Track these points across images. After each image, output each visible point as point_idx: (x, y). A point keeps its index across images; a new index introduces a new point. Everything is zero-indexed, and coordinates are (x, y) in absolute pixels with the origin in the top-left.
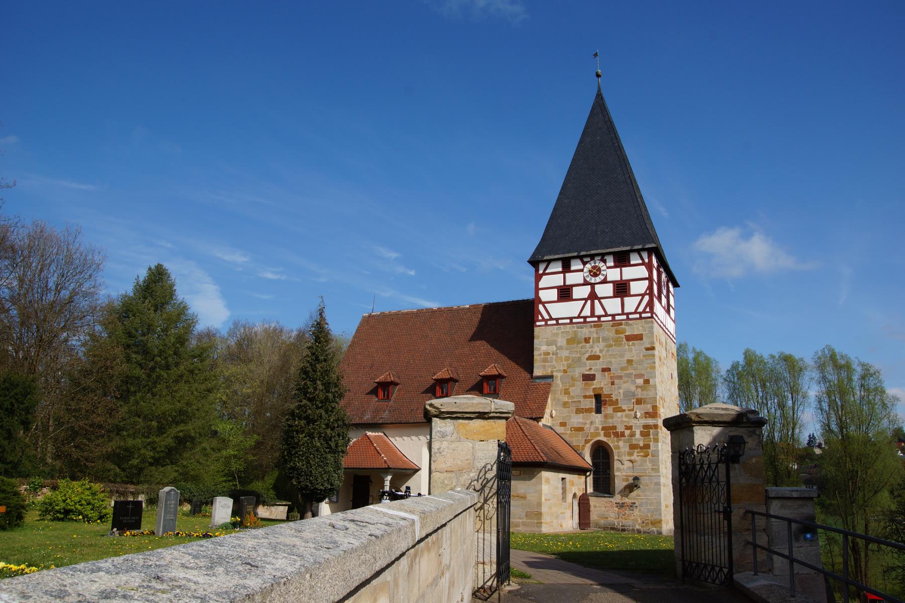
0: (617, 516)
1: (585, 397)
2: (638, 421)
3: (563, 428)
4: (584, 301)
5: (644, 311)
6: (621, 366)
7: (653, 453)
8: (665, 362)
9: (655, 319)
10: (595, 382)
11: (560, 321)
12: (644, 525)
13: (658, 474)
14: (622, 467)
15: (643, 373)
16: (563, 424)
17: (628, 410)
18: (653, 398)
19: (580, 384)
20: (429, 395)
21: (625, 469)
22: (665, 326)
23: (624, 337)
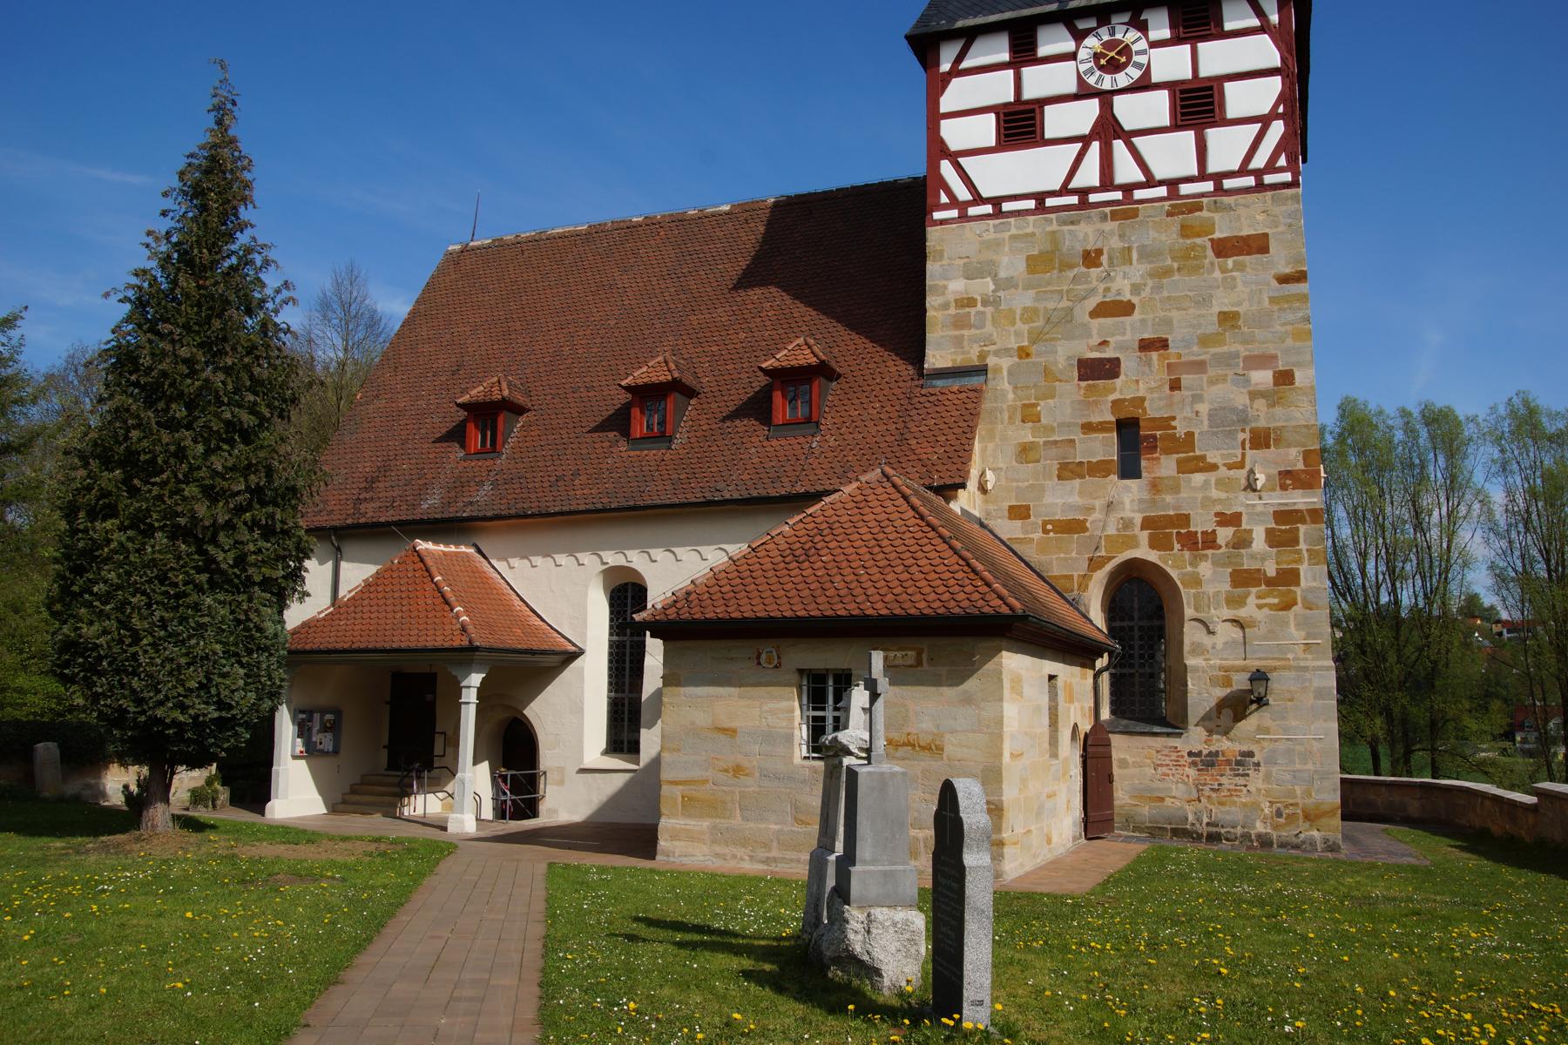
0: (1195, 795)
1: (1088, 428)
2: (1260, 498)
3: (1018, 523)
4: (1080, 145)
5: (1271, 167)
7: (1309, 596)
10: (1118, 382)
11: (1006, 207)
12: (1282, 820)
14: (1207, 641)
15: (1274, 352)
16: (1019, 512)
17: (1225, 465)
18: (1306, 426)
19: (1072, 389)
20: (611, 435)
21: (1219, 646)
23: (1209, 245)
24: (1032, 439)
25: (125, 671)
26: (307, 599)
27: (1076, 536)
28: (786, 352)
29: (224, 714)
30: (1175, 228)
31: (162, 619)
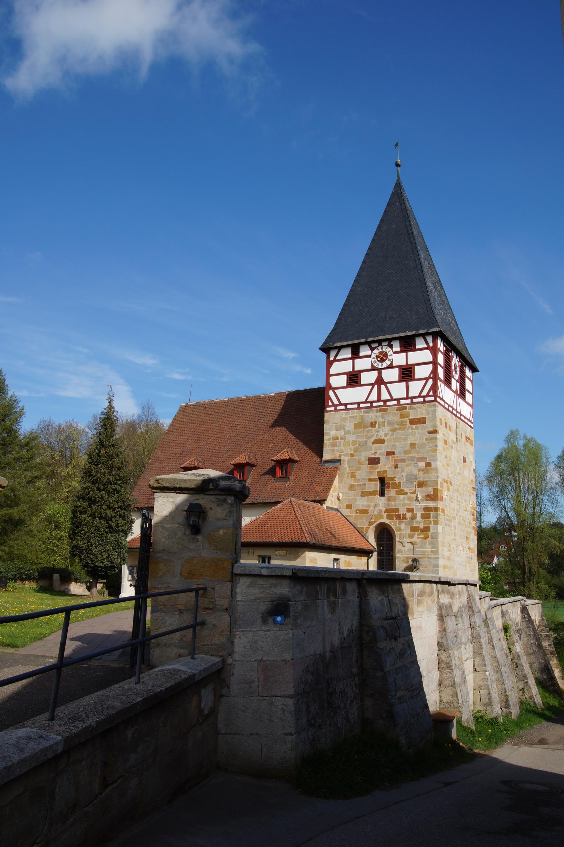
1: (370, 480)
2: (420, 503)
3: (349, 510)
5: (428, 395)
6: (404, 449)
7: (433, 535)
8: (454, 446)
9: (439, 403)
10: (379, 465)
11: (349, 407)
13: (437, 556)
14: (403, 549)
16: (349, 507)
17: (410, 493)
18: (434, 480)
19: (366, 467)
21: (406, 550)
22: (456, 410)
23: (408, 421)
24: (353, 483)
25: (89, 553)
26: (133, 534)
27: (365, 515)
28: (280, 454)
29: (112, 565)
30: (398, 415)
31: (98, 540)
